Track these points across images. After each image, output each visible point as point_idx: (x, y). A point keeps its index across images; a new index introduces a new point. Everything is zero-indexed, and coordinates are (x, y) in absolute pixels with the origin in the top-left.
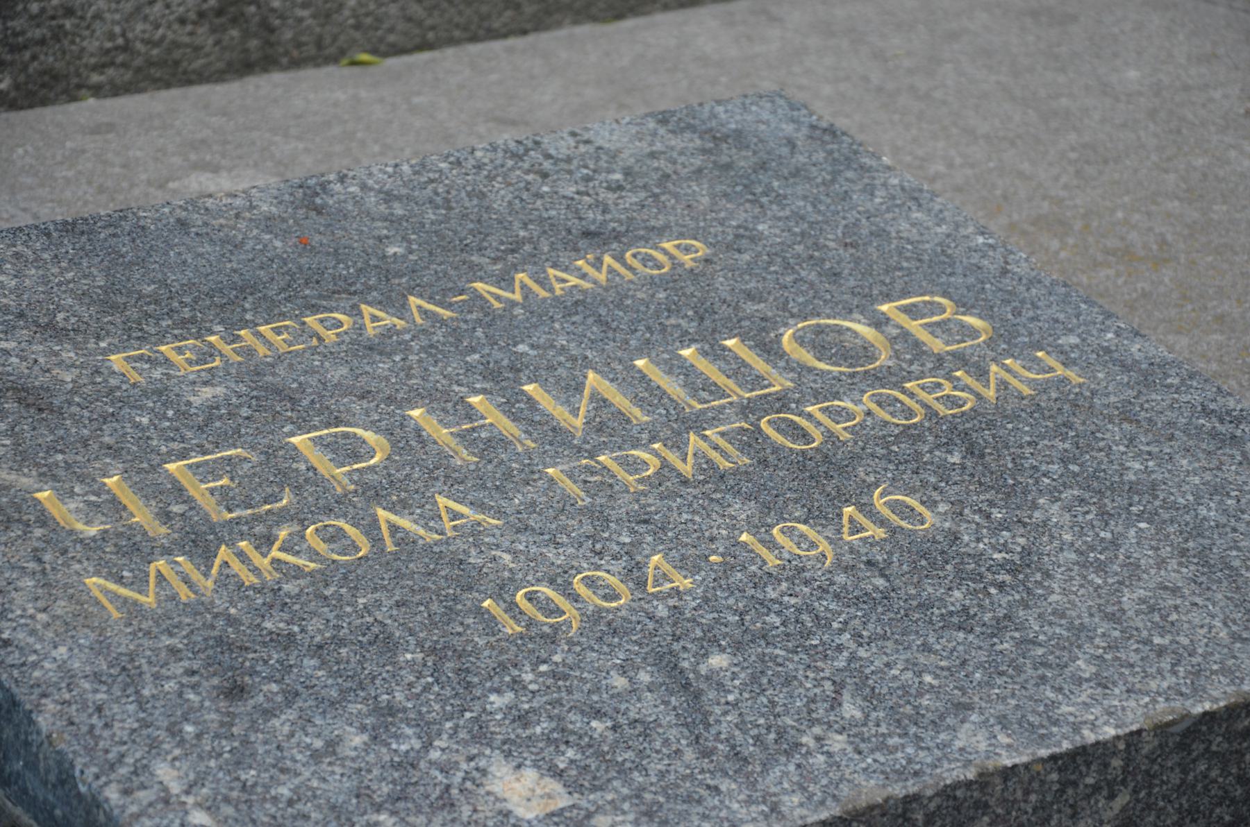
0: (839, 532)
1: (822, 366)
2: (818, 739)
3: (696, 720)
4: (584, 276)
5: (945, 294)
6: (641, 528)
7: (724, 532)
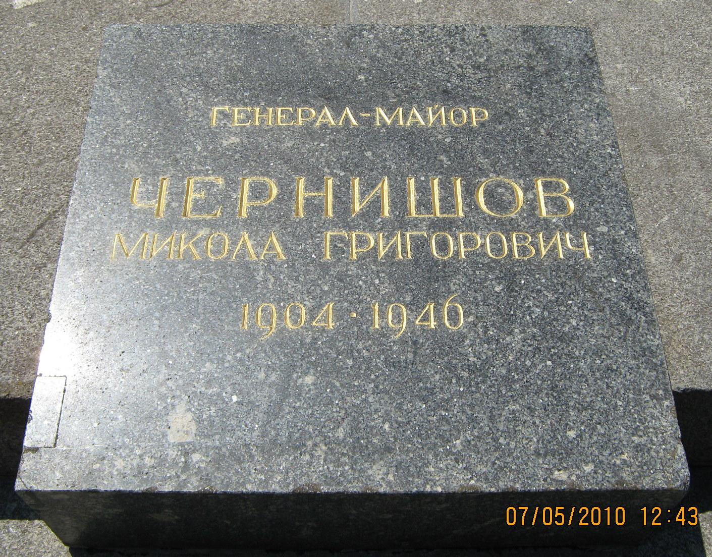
0: (416, 317)
1: (483, 207)
2: (315, 445)
4: (425, 117)
5: (569, 182)
6: (337, 283)
7: (369, 299)
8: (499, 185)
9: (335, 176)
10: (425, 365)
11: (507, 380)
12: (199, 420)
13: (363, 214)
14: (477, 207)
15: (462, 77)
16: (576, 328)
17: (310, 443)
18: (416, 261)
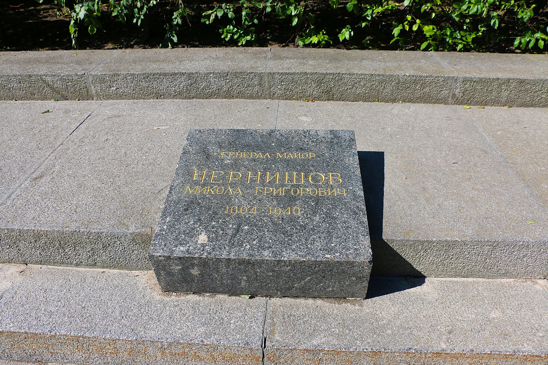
3: (234, 235)
8: (316, 175)
9: (261, 172)
10: (285, 224)
11: (313, 230)
12: (209, 237)
13: (269, 182)
14: (308, 181)
15: (308, 144)
16: (338, 215)
17: (244, 245)
18: (285, 196)
